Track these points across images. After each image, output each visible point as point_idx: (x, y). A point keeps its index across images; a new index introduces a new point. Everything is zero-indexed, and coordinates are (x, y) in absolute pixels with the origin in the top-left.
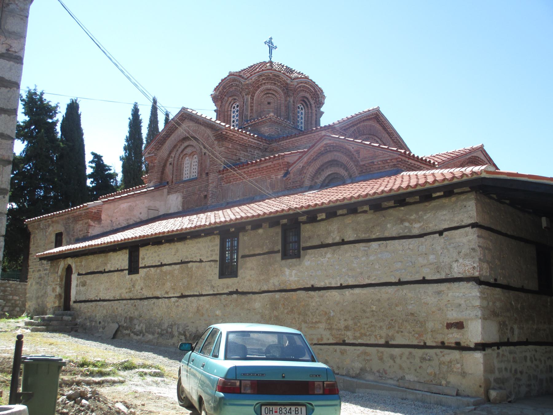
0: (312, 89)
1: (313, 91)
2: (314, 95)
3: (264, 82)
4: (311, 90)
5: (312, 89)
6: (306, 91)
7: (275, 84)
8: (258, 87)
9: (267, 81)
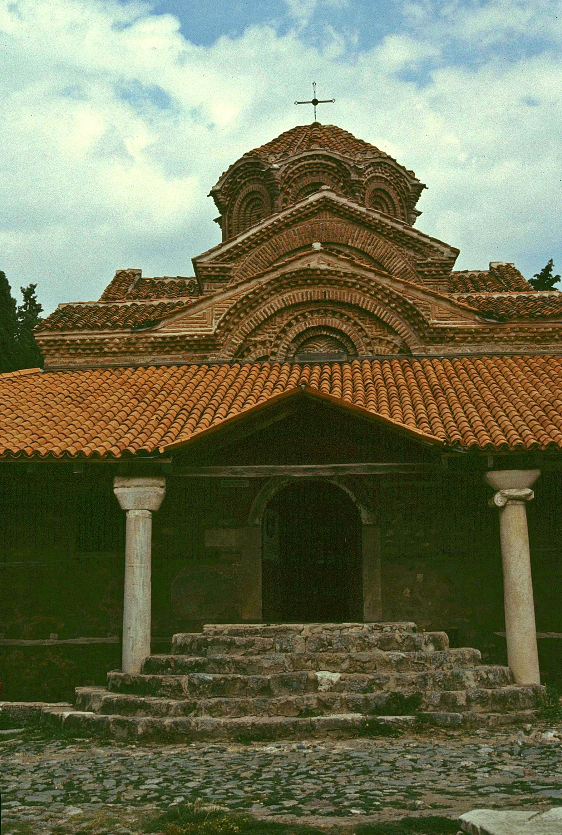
0: (329, 163)
1: (334, 165)
2: (339, 171)
3: (243, 182)
4: (328, 165)
5: (329, 163)
6: (318, 172)
7: (258, 179)
8: (238, 193)
9: (247, 179)
